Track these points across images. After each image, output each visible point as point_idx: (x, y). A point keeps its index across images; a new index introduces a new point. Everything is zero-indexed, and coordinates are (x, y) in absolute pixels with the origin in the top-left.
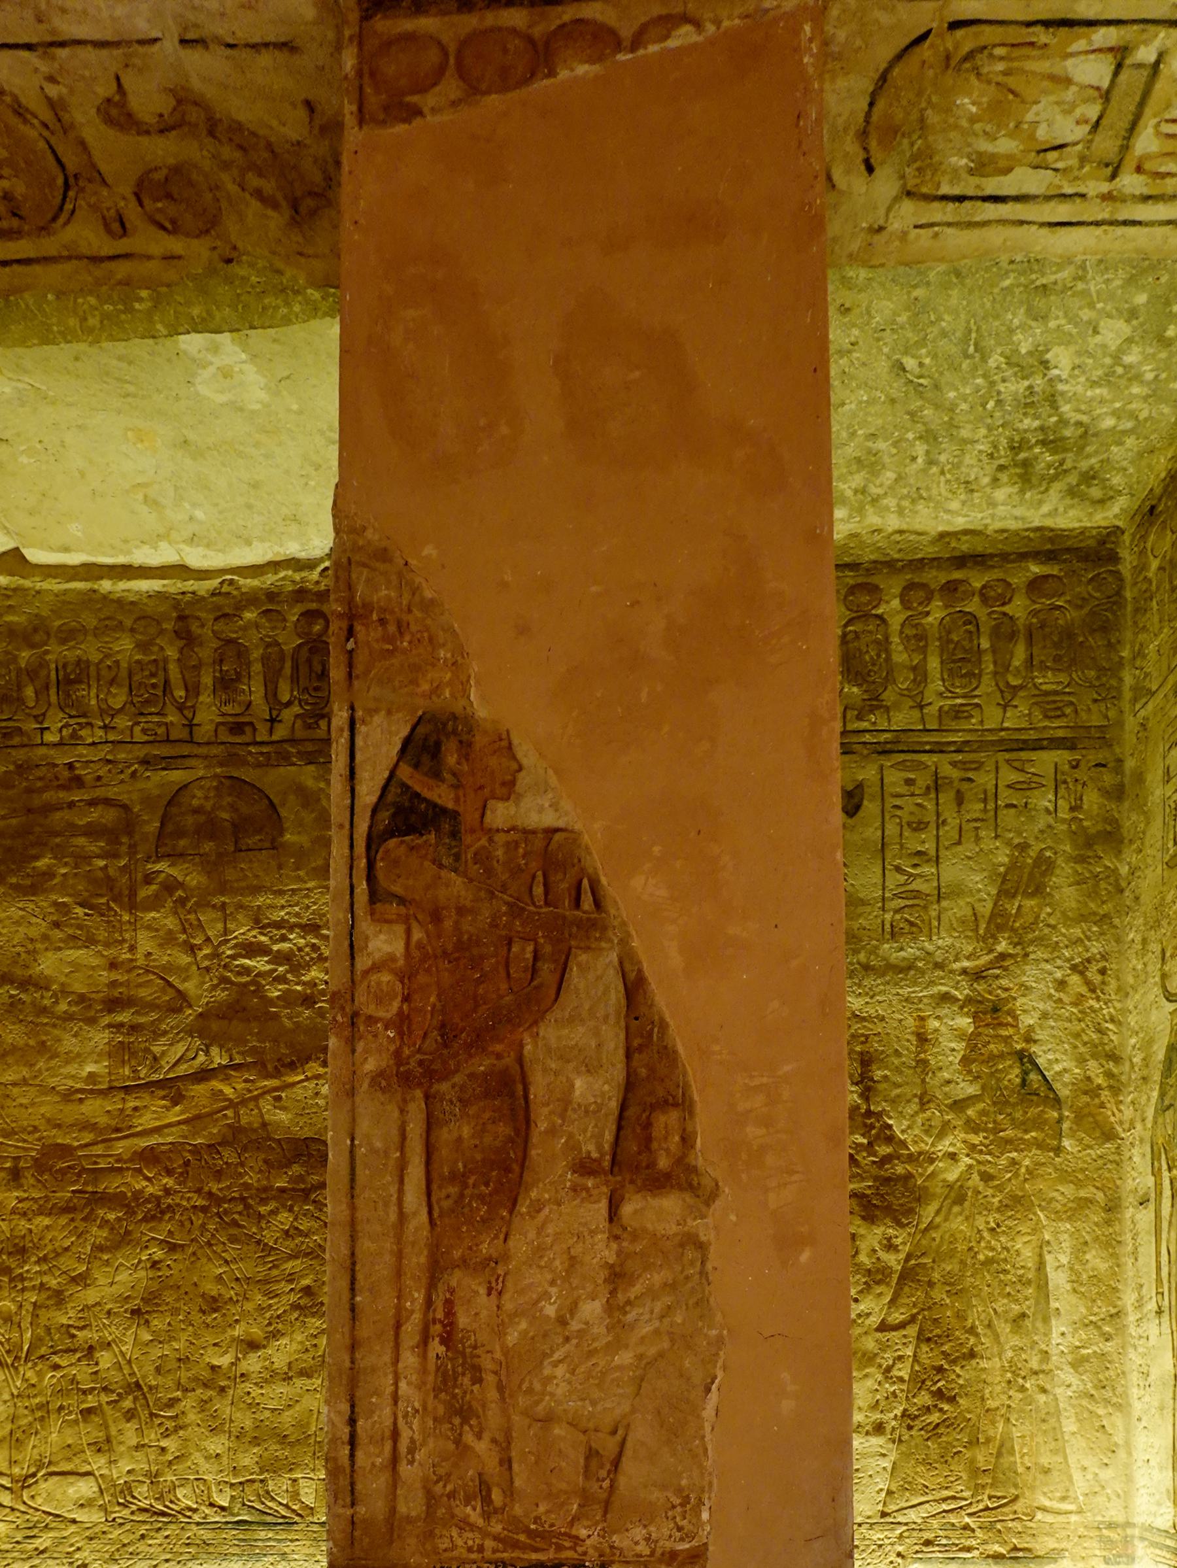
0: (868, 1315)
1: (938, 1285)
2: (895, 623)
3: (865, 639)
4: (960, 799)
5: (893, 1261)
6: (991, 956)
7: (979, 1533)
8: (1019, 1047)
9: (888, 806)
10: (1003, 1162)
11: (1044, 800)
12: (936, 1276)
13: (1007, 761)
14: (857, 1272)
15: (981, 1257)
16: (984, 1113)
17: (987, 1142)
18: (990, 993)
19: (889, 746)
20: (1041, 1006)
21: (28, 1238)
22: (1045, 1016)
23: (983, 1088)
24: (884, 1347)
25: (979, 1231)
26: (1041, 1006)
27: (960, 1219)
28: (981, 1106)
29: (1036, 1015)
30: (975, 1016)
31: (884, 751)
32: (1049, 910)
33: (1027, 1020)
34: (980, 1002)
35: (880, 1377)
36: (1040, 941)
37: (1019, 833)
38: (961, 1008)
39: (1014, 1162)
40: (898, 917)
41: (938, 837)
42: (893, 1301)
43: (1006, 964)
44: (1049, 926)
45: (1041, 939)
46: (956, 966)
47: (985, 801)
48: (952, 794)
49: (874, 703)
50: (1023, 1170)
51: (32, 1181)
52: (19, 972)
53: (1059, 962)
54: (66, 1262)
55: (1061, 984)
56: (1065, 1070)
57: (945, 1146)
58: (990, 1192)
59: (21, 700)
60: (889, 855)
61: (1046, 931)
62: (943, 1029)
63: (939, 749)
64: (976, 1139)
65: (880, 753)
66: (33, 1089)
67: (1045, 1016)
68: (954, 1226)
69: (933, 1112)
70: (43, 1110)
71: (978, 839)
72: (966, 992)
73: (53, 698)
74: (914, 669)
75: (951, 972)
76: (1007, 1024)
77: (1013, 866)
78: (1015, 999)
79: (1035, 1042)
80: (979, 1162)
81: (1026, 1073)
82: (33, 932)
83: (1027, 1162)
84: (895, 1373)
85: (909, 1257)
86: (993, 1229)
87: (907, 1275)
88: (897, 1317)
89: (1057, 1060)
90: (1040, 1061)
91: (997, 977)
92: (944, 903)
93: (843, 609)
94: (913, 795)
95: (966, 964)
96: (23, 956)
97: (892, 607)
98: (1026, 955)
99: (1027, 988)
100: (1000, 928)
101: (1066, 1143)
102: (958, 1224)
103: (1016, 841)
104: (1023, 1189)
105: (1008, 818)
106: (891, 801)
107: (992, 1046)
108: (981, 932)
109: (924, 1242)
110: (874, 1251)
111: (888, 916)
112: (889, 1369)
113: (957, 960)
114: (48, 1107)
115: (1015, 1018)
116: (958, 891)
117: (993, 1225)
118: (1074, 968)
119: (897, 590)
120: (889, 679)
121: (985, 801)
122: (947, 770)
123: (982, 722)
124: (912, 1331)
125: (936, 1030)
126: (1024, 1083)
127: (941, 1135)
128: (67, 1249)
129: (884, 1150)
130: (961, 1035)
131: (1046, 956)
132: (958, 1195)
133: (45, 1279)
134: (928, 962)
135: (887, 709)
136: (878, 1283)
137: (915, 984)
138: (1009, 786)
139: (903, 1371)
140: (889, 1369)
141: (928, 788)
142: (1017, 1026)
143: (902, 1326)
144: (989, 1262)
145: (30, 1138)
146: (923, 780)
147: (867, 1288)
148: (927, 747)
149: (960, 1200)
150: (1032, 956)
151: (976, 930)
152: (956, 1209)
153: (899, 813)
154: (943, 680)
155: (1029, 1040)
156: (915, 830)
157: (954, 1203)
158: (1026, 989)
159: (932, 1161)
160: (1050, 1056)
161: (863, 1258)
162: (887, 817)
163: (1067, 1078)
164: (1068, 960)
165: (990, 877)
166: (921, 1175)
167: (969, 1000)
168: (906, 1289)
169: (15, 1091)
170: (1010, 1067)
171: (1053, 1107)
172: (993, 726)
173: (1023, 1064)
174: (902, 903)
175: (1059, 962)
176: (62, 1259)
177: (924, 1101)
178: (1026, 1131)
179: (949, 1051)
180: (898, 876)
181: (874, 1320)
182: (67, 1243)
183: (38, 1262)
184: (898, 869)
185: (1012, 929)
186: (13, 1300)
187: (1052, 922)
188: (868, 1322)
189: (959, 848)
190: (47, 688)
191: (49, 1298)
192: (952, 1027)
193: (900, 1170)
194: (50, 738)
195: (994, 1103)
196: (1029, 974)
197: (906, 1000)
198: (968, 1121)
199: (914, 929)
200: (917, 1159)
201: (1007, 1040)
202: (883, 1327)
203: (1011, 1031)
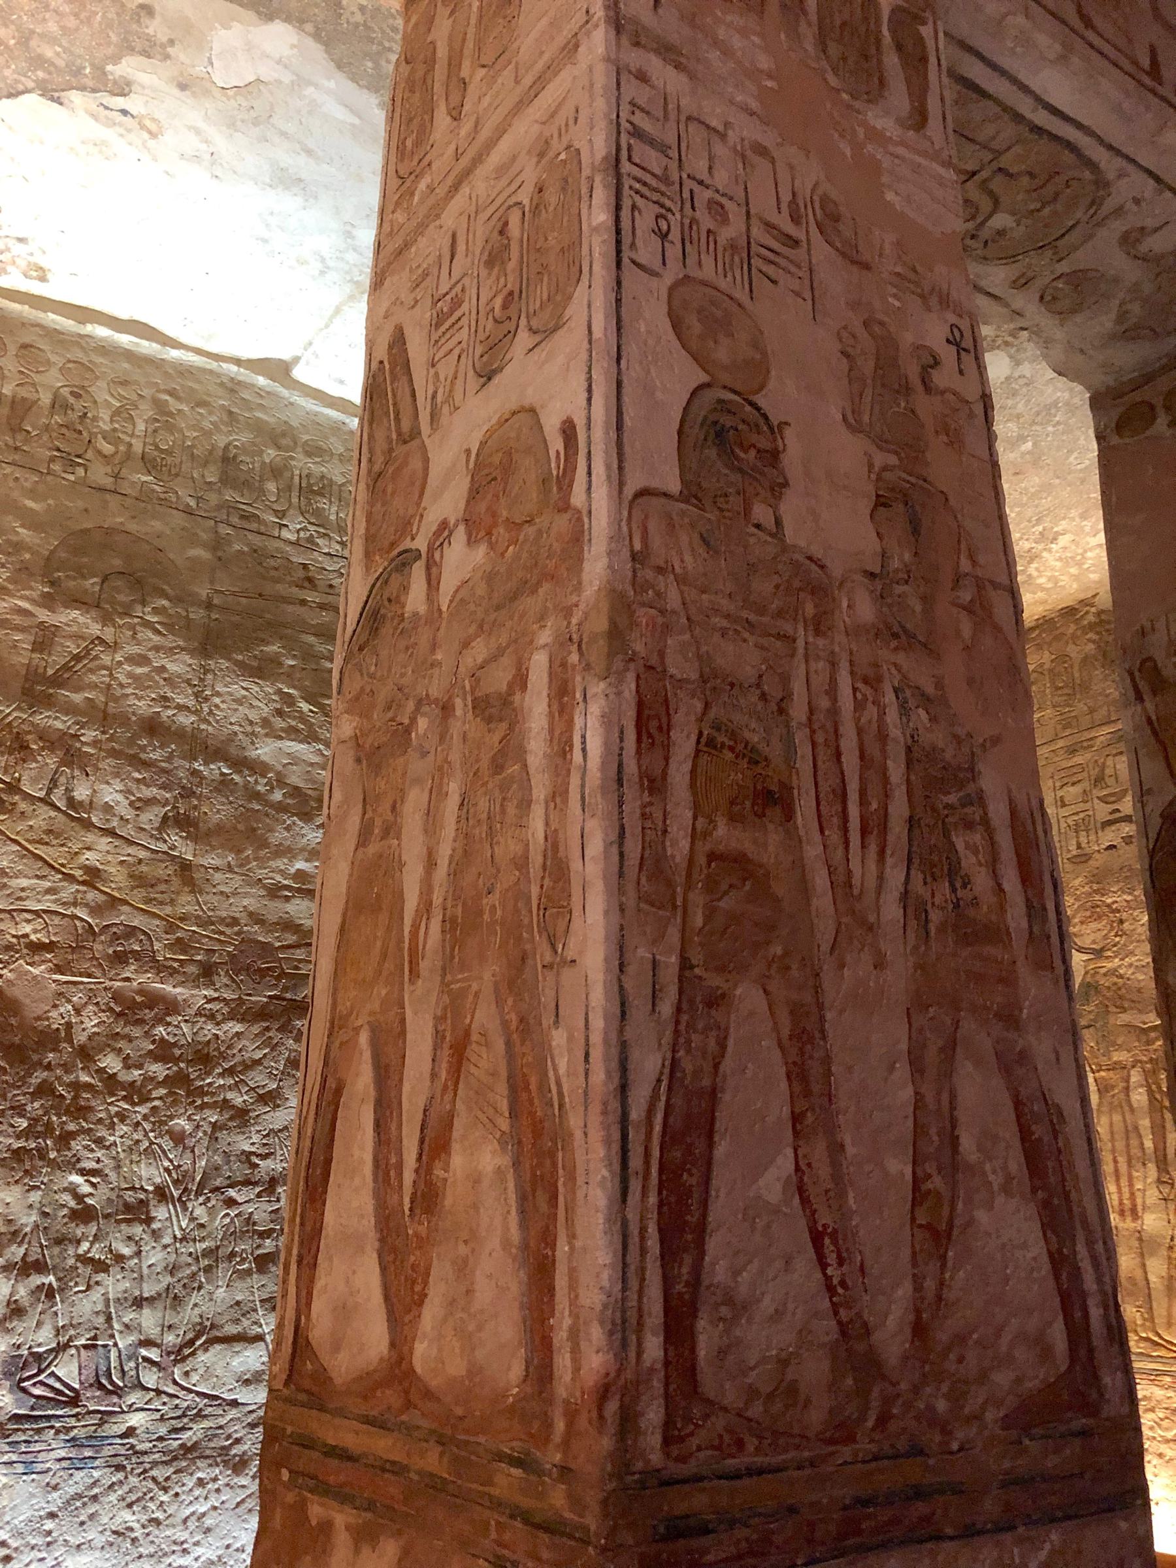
21: (213, 1046)
51: (225, 980)
52: (233, 751)
54: (257, 1078)
59: (262, 491)
66: (238, 878)
70: (245, 902)
73: (295, 500)
82: (253, 715)
96: (241, 736)
114: (252, 901)
128: (258, 1062)
133: (230, 1095)
145: (228, 931)
169: (218, 876)
176: (251, 1074)
182: (258, 1055)
183: (222, 1075)
186: (189, 1119)
190: (289, 488)
191: (231, 1119)
194: (285, 534)
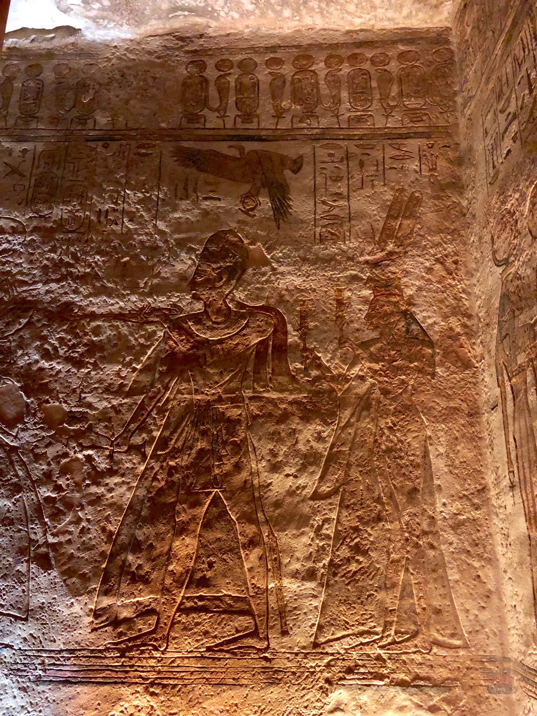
0: (304, 487)
1: (354, 467)
2: (322, 75)
3: (305, 82)
4: (362, 164)
5: (323, 448)
6: (384, 253)
7: (389, 664)
8: (403, 308)
9: (318, 168)
10: (396, 382)
11: (414, 166)
12: (352, 459)
13: (390, 144)
14: (296, 456)
15: (383, 447)
16: (381, 349)
17: (385, 368)
18: (383, 275)
19: (318, 136)
20: (417, 283)
22: (420, 289)
23: (381, 334)
24: (316, 511)
25: (381, 429)
26: (417, 283)
27: (368, 420)
28: (379, 345)
29: (414, 289)
30: (374, 289)
31: (316, 139)
32: (419, 226)
33: (409, 292)
34: (378, 281)
35: (312, 534)
36: (414, 244)
37: (399, 183)
38: (365, 284)
39: (403, 382)
40: (324, 230)
41: (348, 185)
42: (322, 478)
43: (393, 258)
44: (420, 235)
45: (415, 243)
46: (361, 259)
47: (377, 165)
48: (357, 162)
49: (310, 113)
50: (410, 387)
53: (427, 257)
55: (429, 270)
56: (435, 323)
57: (356, 370)
58: (388, 402)
60: (318, 195)
61: (419, 238)
62: (354, 297)
63: (349, 138)
64: (377, 367)
65: (312, 140)
67: (420, 289)
68: (363, 425)
69: (347, 347)
71: (373, 186)
72: (368, 274)
74: (333, 97)
75: (358, 262)
76: (395, 295)
77: (395, 201)
78: (400, 279)
79: (414, 305)
80: (379, 382)
81: (409, 324)
83: (412, 382)
84: (324, 531)
85: (333, 446)
86: (390, 428)
87: (332, 458)
88: (325, 489)
89: (428, 316)
90: (418, 317)
91: (388, 265)
92: (353, 222)
93: (292, 67)
94: (333, 162)
95: (368, 258)
97: (320, 67)
98: (406, 252)
99: (407, 272)
100: (390, 237)
101: (438, 370)
102: (366, 424)
103: (397, 187)
104: (410, 400)
105: (392, 175)
106: (320, 165)
107: (386, 308)
108: (377, 239)
109: (343, 435)
110: (308, 441)
111: (318, 230)
112: (320, 528)
113: (362, 255)
115: (401, 290)
116: (362, 215)
117: (390, 424)
118: (437, 260)
119: (323, 58)
120: (319, 101)
121: (377, 165)
122: (353, 149)
123: (374, 125)
124: (336, 500)
125: (349, 298)
126: (407, 331)
127: (352, 365)
129: (314, 373)
130: (365, 301)
131: (419, 253)
132: (365, 404)
134: (343, 257)
135: (317, 117)
136: (311, 464)
137: (334, 269)
138: (391, 158)
139: (329, 530)
140: (320, 528)
141: (342, 158)
142: (402, 296)
143: (328, 496)
144: (389, 450)
146: (339, 154)
147: (303, 469)
148: (342, 137)
149: (367, 407)
150: (410, 253)
151: (373, 237)
152: (365, 413)
153: (324, 171)
154: (350, 103)
155: (410, 303)
156: (334, 181)
157: (363, 409)
158: (407, 273)
159: (347, 381)
160: (425, 314)
161: (301, 446)
162: (317, 174)
163: (437, 328)
164: (433, 256)
165: (381, 207)
166: (340, 390)
167: (370, 279)
168: (331, 468)
170: (398, 320)
171: (428, 346)
172: (381, 126)
173: (406, 319)
174: (326, 222)
175: (427, 257)
177: (342, 342)
178: (411, 362)
179: (358, 311)
180: (324, 207)
181: (309, 491)
184: (324, 202)
185: (396, 237)
187: (422, 233)
188: (304, 493)
189: (362, 191)
192: (359, 296)
193: (325, 386)
195: (388, 343)
196: (408, 264)
197: (329, 279)
198: (371, 354)
199: (334, 237)
200: (338, 379)
201: (396, 304)
202: (316, 496)
203: (398, 298)
